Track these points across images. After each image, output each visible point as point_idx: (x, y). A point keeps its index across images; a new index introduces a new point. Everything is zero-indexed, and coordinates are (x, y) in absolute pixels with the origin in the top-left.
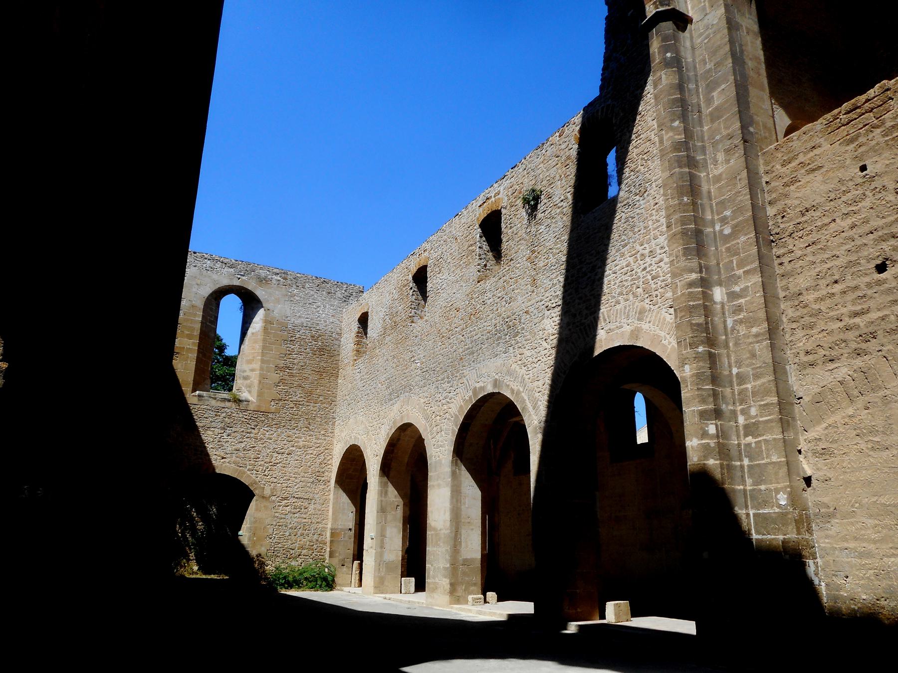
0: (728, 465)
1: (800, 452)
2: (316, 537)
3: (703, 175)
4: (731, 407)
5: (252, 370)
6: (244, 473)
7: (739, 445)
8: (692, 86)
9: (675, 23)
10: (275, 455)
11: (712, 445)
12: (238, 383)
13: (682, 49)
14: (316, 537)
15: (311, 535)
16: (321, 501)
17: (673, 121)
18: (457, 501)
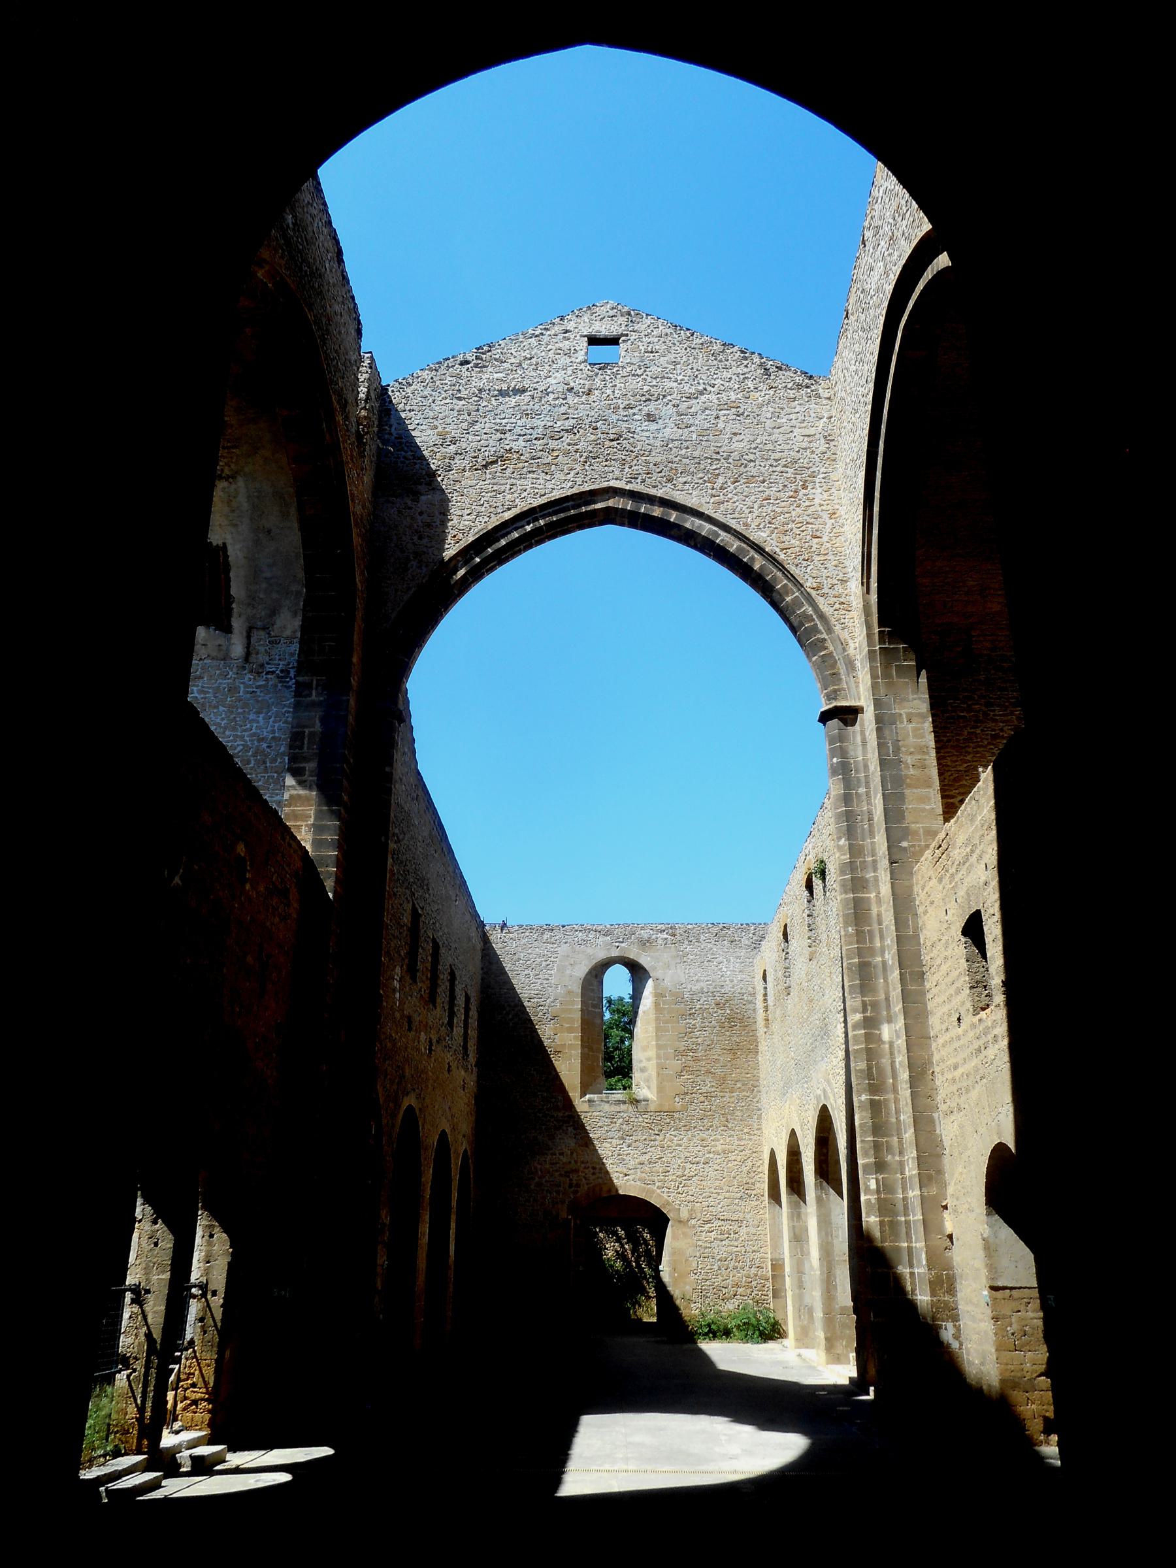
0: (891, 1222)
1: (945, 1207)
2: (753, 1270)
3: (873, 895)
4: (897, 1158)
5: (649, 1059)
6: (653, 1192)
7: (905, 1199)
8: (862, 790)
9: (840, 720)
10: (688, 1165)
11: (873, 1201)
12: (637, 1075)
13: (851, 747)
14: (753, 1270)
15: (747, 1268)
16: (756, 1223)
17: (839, 839)
18: (827, 1234)
